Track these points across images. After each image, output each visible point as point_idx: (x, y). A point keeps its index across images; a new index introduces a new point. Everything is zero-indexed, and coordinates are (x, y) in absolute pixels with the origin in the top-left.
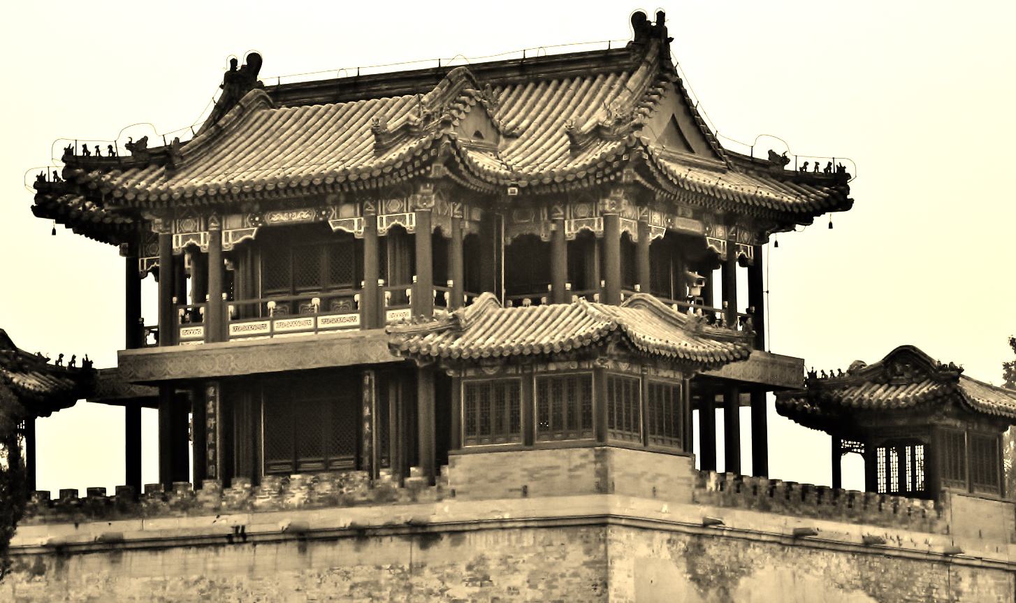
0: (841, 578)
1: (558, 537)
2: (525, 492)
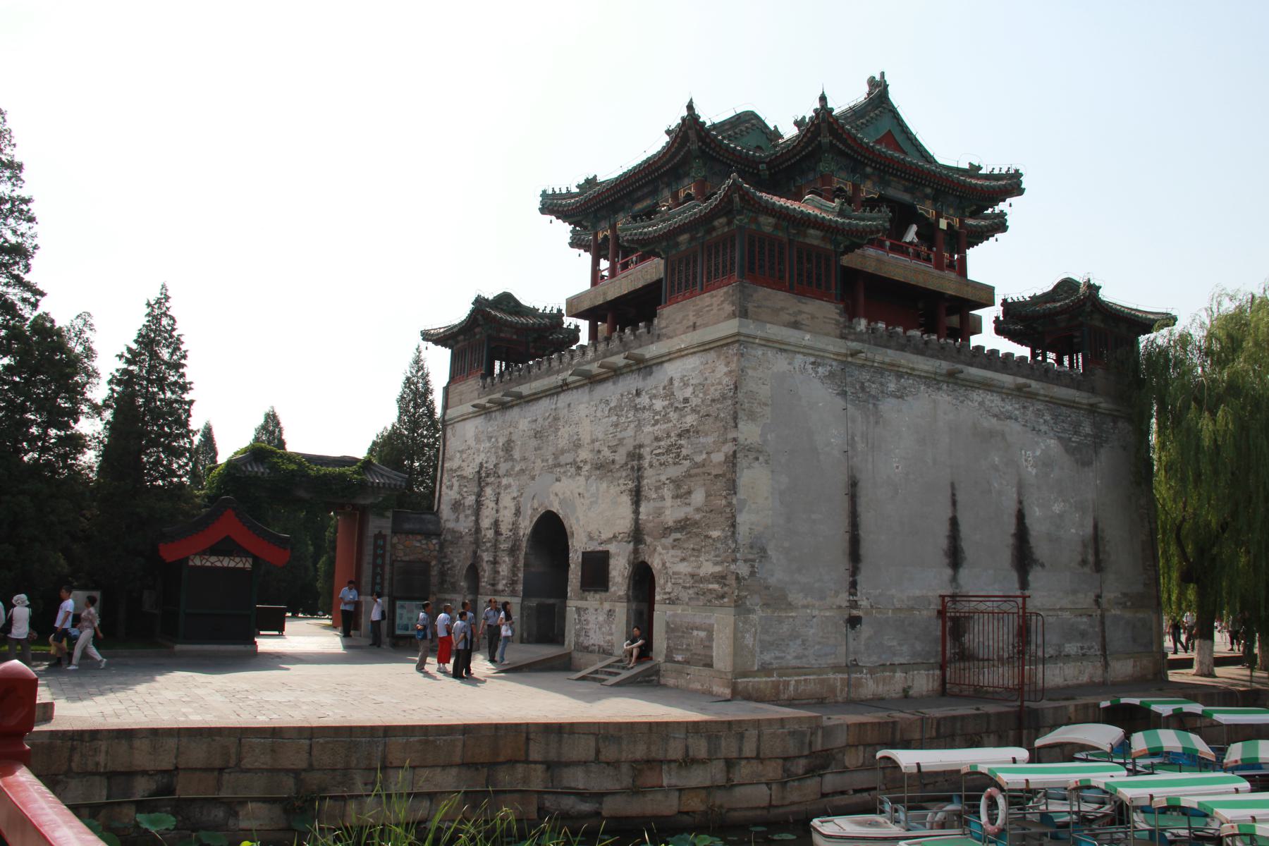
0: (996, 410)
1: (712, 354)
2: (694, 327)
